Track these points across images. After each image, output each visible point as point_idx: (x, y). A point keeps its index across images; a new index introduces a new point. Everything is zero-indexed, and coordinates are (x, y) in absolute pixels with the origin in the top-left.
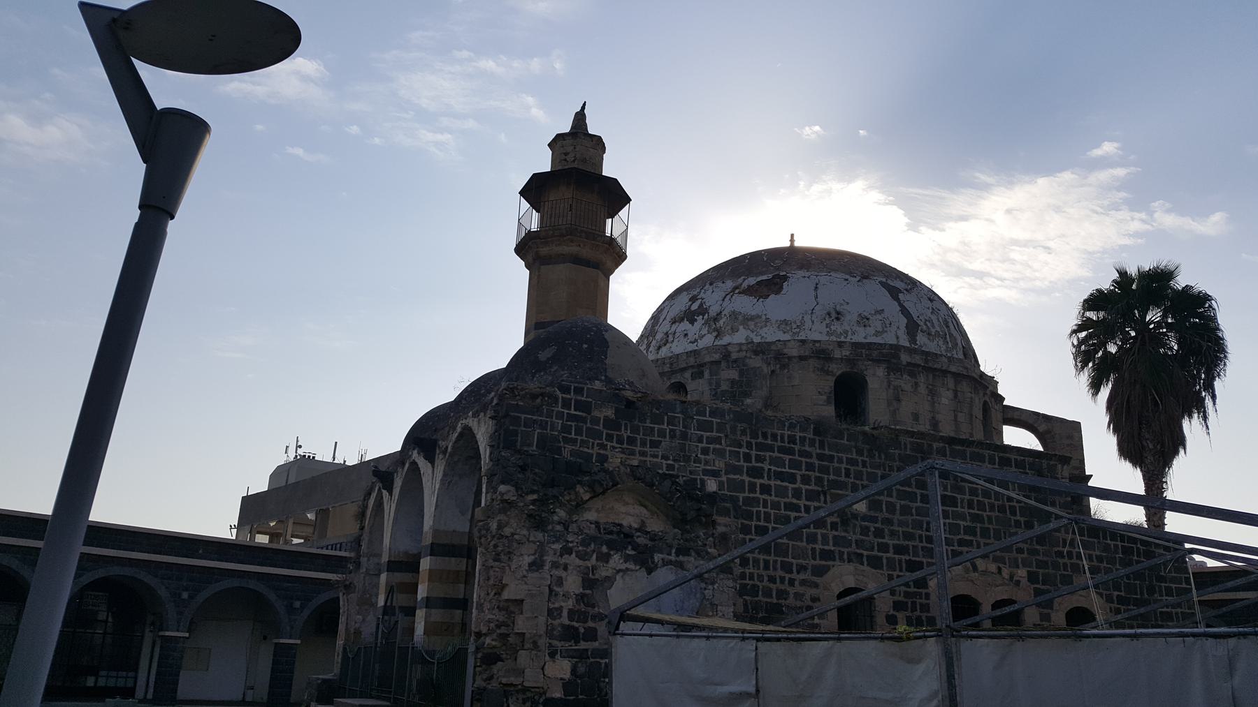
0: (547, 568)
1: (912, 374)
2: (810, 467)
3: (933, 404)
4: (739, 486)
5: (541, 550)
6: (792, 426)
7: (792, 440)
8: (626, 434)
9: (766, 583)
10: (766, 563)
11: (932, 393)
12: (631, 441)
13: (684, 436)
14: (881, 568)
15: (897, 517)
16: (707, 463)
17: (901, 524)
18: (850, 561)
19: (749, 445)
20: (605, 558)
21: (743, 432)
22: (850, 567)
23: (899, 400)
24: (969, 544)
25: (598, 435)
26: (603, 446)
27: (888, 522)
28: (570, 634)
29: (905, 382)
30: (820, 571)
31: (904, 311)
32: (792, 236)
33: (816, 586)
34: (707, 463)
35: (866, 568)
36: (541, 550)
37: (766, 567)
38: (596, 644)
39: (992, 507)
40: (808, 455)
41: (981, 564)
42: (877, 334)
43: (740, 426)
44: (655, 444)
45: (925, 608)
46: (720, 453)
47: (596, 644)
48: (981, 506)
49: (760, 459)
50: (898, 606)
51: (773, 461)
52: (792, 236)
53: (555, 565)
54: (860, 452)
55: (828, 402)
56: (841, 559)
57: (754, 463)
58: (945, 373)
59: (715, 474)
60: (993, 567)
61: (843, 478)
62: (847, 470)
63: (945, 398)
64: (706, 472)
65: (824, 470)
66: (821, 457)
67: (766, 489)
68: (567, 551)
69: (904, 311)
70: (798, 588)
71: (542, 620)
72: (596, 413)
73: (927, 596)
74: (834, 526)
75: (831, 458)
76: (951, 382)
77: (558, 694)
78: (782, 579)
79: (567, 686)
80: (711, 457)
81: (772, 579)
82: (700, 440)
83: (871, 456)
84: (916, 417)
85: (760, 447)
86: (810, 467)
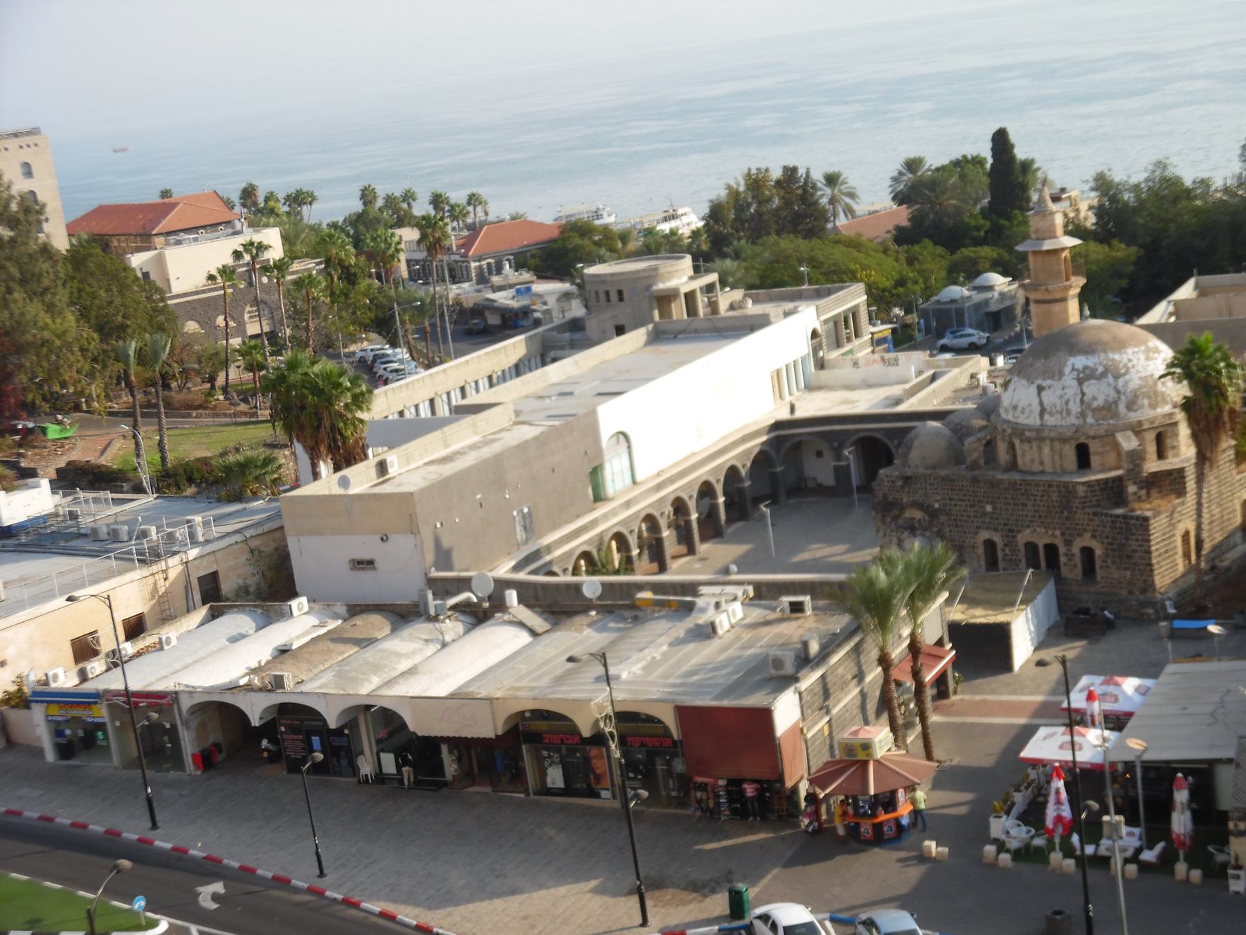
11: (1040, 449)
29: (1026, 446)
30: (976, 533)
31: (1041, 403)
41: (1038, 529)
50: (1005, 545)
63: (1046, 450)
69: (1041, 403)
76: (1048, 442)
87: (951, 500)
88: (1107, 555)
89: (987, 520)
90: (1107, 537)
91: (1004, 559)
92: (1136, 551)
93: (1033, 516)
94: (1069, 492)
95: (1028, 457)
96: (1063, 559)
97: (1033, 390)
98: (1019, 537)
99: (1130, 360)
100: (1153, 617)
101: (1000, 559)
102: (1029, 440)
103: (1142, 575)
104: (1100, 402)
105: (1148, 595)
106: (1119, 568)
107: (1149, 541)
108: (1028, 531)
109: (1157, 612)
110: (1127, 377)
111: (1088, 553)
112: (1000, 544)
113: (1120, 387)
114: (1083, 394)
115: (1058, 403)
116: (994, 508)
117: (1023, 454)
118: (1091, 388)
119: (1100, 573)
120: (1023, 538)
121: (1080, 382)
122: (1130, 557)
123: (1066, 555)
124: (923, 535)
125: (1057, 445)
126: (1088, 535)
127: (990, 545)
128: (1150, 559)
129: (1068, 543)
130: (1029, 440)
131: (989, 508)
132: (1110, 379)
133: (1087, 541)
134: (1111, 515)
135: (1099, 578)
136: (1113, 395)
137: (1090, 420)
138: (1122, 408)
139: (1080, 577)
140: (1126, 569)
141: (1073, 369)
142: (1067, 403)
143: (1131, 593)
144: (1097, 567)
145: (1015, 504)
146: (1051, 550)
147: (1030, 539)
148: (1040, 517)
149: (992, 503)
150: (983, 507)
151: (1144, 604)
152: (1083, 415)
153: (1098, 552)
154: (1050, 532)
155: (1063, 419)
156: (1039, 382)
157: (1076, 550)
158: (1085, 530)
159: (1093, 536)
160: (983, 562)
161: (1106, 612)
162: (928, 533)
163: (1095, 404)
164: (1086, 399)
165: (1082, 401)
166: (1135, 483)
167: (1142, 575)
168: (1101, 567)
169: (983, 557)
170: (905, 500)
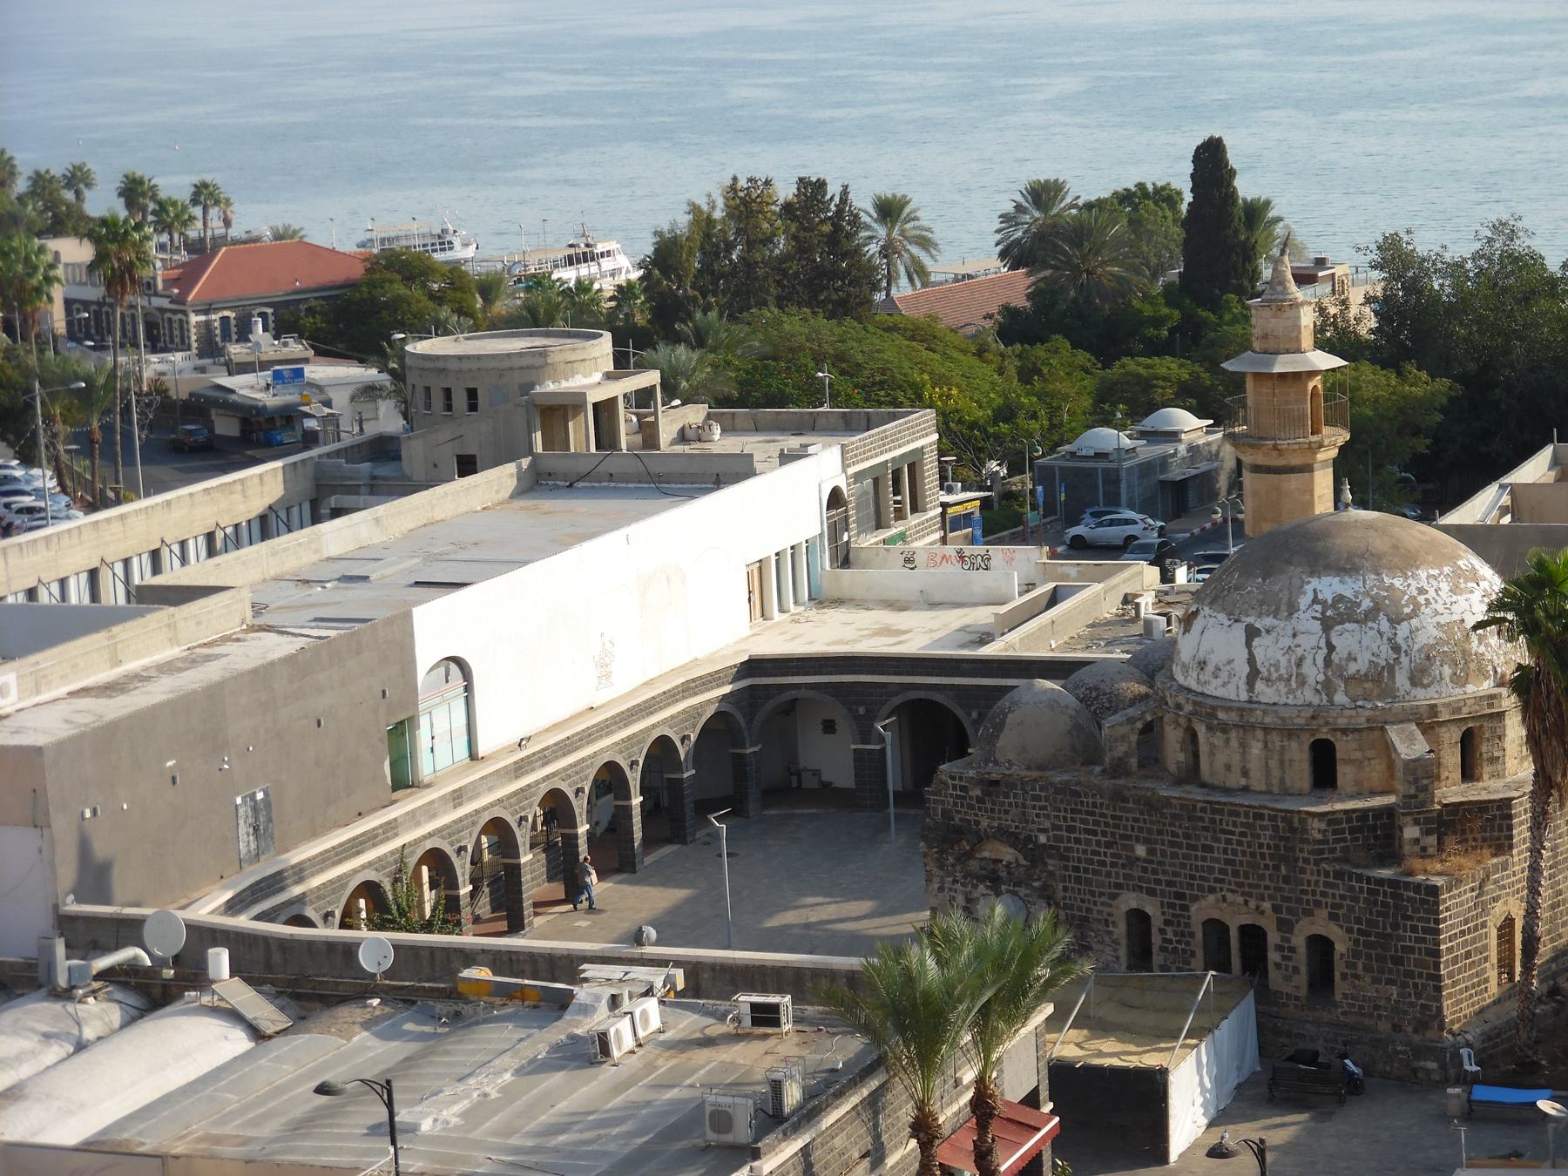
1: (1224, 731)
2: (1107, 824)
3: (1244, 754)
4: (1059, 839)
5: (942, 882)
6: (1094, 796)
8: (989, 806)
12: (992, 811)
13: (1024, 806)
15: (1168, 860)
17: (1171, 865)
20: (975, 887)
22: (1134, 895)
24: (1222, 881)
25: (971, 807)
27: (1160, 863)
29: (1218, 739)
30: (1114, 897)
31: (1251, 660)
36: (942, 882)
39: (1244, 853)
40: (1103, 815)
41: (1230, 896)
42: (1224, 685)
44: (1006, 812)
45: (1187, 925)
46: (1047, 817)
48: (1235, 852)
50: (1167, 922)
51: (1083, 821)
54: (1142, 813)
58: (1253, 727)
59: (1044, 831)
60: (1240, 900)
63: (1256, 749)
64: (1040, 830)
65: (1117, 826)
66: (1114, 817)
67: (1077, 841)
68: (955, 881)
69: (1251, 660)
70: (1099, 907)
74: (1124, 866)
75: (1120, 818)
76: (1259, 734)
81: (1083, 901)
83: (1150, 814)
85: (1073, 811)
87: (1071, 829)
88: (1356, 954)
89: (1137, 873)
90: (1358, 921)
91: (1162, 949)
92: (1411, 950)
93: (1222, 871)
94: (1292, 830)
95: (1221, 759)
96: (1273, 956)
97: (1239, 632)
98: (1194, 908)
99: (1422, 591)
100: (1436, 1077)
101: (1155, 949)
102: (1224, 728)
103: (1418, 995)
104: (1361, 666)
105: (1429, 1034)
106: (1376, 981)
107: (1438, 932)
108: (1211, 898)
109: (1443, 1067)
110: (1414, 622)
111: (1321, 947)
112: (1157, 922)
113: (1399, 640)
114: (1331, 648)
115: (1283, 661)
116: (1151, 851)
117: (1212, 754)
118: (1347, 639)
119: (1341, 987)
120: (1202, 909)
121: (1327, 625)
122: (1398, 961)
123: (1279, 948)
124: (1015, 893)
125: (1276, 740)
126: (1324, 913)
127: (1138, 920)
128: (1437, 966)
129: (1286, 927)
130: (1224, 728)
131: (1141, 851)
132: (1384, 625)
133: (1321, 924)
134: (1369, 880)
135: (1338, 997)
136: (1386, 652)
137: (1340, 698)
138: (1402, 680)
139: (1303, 992)
140: (1390, 982)
141: (1315, 601)
142: (1299, 664)
143: (1397, 1028)
144: (1337, 976)
146: (1253, 937)
147: (1216, 915)
148: (1236, 874)
149: (1146, 841)
150: (1133, 851)
151: (1421, 1052)
152: (1328, 687)
153: (1340, 947)
154: (1252, 904)
155: (1291, 691)
156: (1250, 620)
157: (1299, 940)
158: (1318, 904)
159: (1333, 917)
160: (1123, 952)
161: (1347, 1061)
162: (1022, 891)
163: (1352, 668)
164: (1334, 656)
165: (1328, 662)
166: (1417, 822)
167: (1418, 995)
168: (1344, 977)
169: (1124, 942)
170: (984, 823)
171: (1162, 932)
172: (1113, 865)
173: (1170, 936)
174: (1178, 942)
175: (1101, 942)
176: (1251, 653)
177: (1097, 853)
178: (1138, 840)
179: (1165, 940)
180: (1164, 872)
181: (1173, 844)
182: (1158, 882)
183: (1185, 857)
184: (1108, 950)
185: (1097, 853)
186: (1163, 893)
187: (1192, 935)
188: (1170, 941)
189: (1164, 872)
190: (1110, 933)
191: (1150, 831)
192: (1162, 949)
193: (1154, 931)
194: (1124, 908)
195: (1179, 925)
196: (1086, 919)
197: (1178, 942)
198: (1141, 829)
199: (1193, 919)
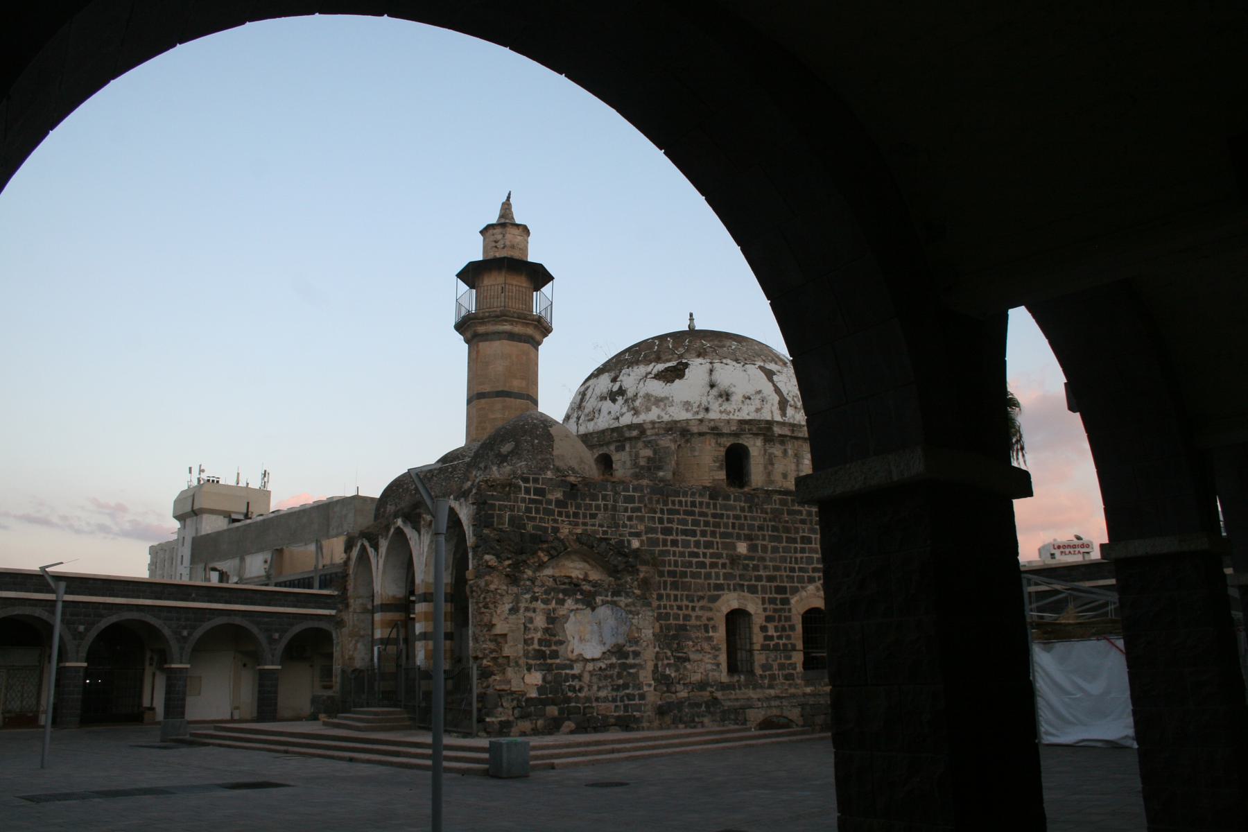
0: (522, 611)
1: (782, 443)
2: (707, 524)
4: (654, 542)
5: (517, 599)
6: (693, 494)
7: (693, 504)
8: (572, 510)
9: (675, 611)
10: (676, 596)
12: (576, 515)
13: (614, 508)
14: (756, 592)
15: (769, 555)
16: (631, 527)
17: (772, 560)
18: (735, 590)
19: (662, 511)
20: (561, 602)
21: (658, 502)
22: (735, 595)
23: (772, 464)
25: (551, 513)
26: (555, 521)
27: (763, 559)
28: (540, 655)
29: (777, 450)
30: (714, 599)
31: (777, 390)
32: (691, 315)
33: (711, 609)
34: (631, 527)
35: (746, 594)
36: (517, 599)
37: (676, 600)
38: (558, 661)
42: (758, 410)
43: (655, 498)
45: (788, 619)
46: (641, 519)
47: (558, 661)
49: (670, 521)
50: (769, 619)
52: (691, 315)
53: (527, 609)
55: (720, 468)
56: (729, 590)
57: (666, 525)
59: (637, 535)
61: (730, 530)
62: (733, 524)
64: (631, 534)
65: (717, 525)
66: (714, 516)
67: (675, 543)
68: (535, 599)
69: (777, 390)
71: (520, 646)
72: (550, 497)
73: (790, 610)
77: (534, 694)
78: (687, 607)
79: (540, 689)
80: (635, 522)
81: (680, 608)
82: (626, 510)
84: (785, 476)
85: (670, 512)
86: (707, 524)
87: (667, 531)
91: (765, 648)
116: (752, 548)
124: (614, 603)
130: (783, 439)
131: (742, 548)
145: (789, 540)
149: (748, 538)
150: (734, 548)
162: (623, 601)
170: (565, 531)
171: (764, 629)
172: (713, 565)
173: (771, 632)
174: (780, 637)
175: (701, 651)
176: (774, 385)
177: (696, 555)
178: (739, 538)
179: (767, 638)
180: (766, 568)
181: (773, 539)
182: (759, 578)
183: (786, 550)
184: (707, 658)
185: (696, 555)
186: (764, 589)
187: (792, 628)
188: (771, 638)
189: (766, 568)
190: (710, 639)
191: (751, 527)
192: (765, 648)
193: (756, 629)
194: (725, 610)
195: (780, 620)
196: (683, 628)
197: (780, 637)
198: (741, 527)
199: (794, 611)
